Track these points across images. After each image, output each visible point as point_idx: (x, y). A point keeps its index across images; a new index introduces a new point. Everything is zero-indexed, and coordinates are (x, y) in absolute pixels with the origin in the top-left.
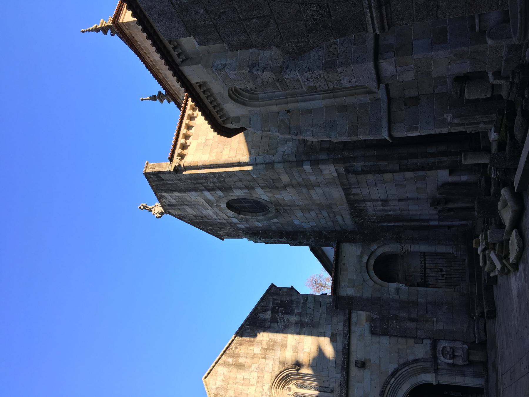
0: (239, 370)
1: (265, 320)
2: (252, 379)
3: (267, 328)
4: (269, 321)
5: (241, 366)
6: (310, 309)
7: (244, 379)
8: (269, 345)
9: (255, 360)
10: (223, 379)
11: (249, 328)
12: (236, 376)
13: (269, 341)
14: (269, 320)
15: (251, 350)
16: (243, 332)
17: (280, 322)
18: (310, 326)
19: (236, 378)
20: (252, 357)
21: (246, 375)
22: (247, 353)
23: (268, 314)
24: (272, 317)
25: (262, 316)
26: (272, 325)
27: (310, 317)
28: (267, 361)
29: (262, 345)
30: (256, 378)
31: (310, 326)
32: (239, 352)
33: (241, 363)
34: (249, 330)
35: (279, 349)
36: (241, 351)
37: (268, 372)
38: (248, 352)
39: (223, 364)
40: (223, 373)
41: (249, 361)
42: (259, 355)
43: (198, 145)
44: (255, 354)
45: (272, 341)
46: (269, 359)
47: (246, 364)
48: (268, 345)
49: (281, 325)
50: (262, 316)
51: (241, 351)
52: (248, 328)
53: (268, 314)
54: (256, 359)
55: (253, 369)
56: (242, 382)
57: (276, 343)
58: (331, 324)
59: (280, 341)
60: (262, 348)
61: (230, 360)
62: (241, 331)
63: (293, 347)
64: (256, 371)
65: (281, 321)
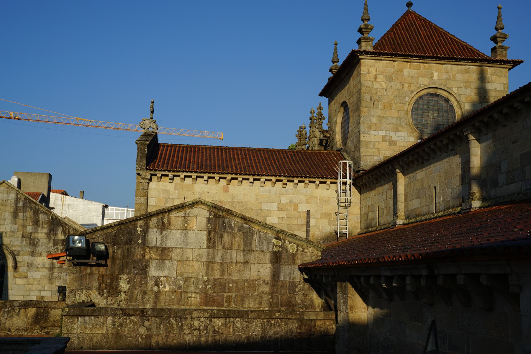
0: (12, 214)
1: (56, 234)
2: (5, 226)
3: (49, 236)
4: (55, 238)
5: (15, 215)
6: (66, 276)
7: (5, 219)
8: (34, 239)
9: (21, 228)
10: (5, 200)
11: (49, 218)
12: (7, 211)
13: (38, 239)
14: (56, 238)
15: (30, 223)
16: (46, 213)
17: (54, 248)
18: (51, 277)
19: (6, 212)
20: (23, 225)
21: (8, 221)
22: (26, 220)
23: (61, 236)
24: (59, 240)
25: (59, 230)
26: (52, 241)
27: (59, 276)
28: (20, 239)
29: (34, 234)
30: (6, 231)
31: (50, 276)
32: (28, 212)
33: (18, 215)
34: (47, 219)
35: (30, 250)
36: (28, 214)
37: (11, 241)
38: (28, 221)
39: (18, 197)
40: (10, 198)
41: (20, 222)
42: (25, 231)
43: (168, 192)
44: (26, 227)
45: (37, 242)
46: (22, 241)
47: (17, 220)
48: (34, 239)
49: (51, 249)
50: (60, 230)
51: (28, 214)
52: (49, 218)
53: (61, 236)
54: (22, 229)
55: (13, 226)
56: (2, 218)
57: (36, 246)
58: (51, 295)
59: (38, 250)
60: (31, 233)
61: (21, 204)
62: (47, 212)
63: (32, 262)
64: (12, 230)
65: (55, 249)
